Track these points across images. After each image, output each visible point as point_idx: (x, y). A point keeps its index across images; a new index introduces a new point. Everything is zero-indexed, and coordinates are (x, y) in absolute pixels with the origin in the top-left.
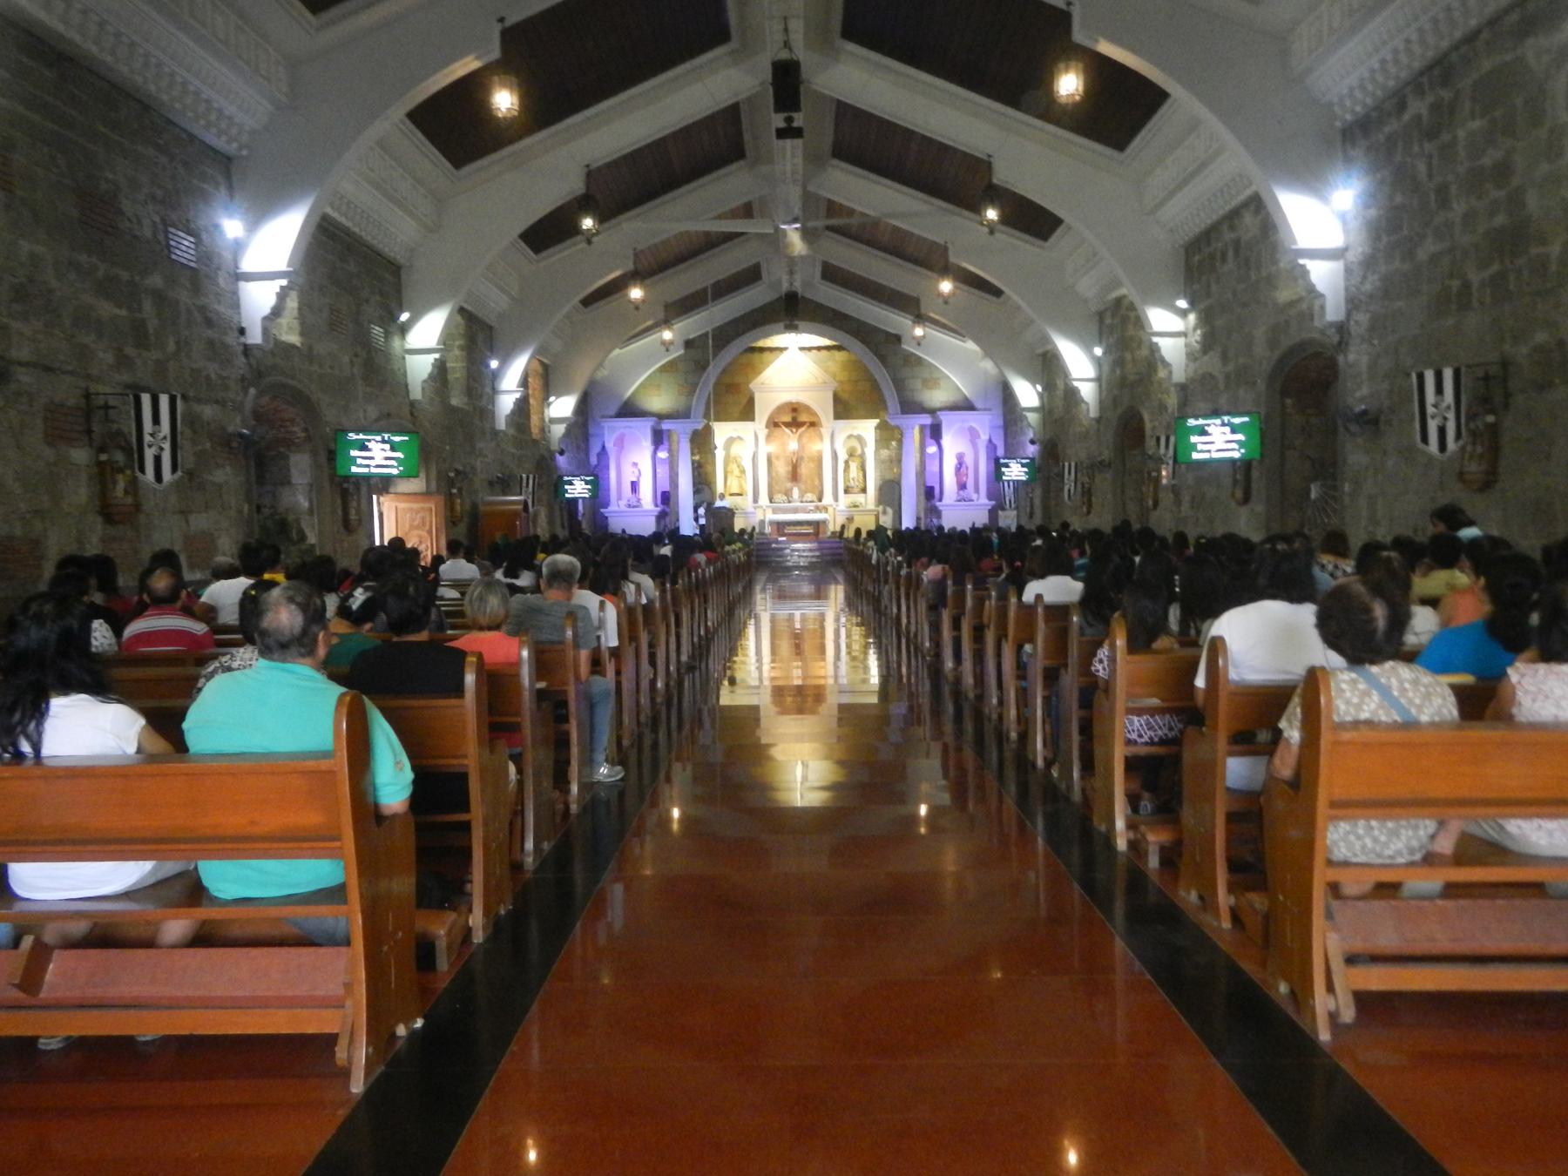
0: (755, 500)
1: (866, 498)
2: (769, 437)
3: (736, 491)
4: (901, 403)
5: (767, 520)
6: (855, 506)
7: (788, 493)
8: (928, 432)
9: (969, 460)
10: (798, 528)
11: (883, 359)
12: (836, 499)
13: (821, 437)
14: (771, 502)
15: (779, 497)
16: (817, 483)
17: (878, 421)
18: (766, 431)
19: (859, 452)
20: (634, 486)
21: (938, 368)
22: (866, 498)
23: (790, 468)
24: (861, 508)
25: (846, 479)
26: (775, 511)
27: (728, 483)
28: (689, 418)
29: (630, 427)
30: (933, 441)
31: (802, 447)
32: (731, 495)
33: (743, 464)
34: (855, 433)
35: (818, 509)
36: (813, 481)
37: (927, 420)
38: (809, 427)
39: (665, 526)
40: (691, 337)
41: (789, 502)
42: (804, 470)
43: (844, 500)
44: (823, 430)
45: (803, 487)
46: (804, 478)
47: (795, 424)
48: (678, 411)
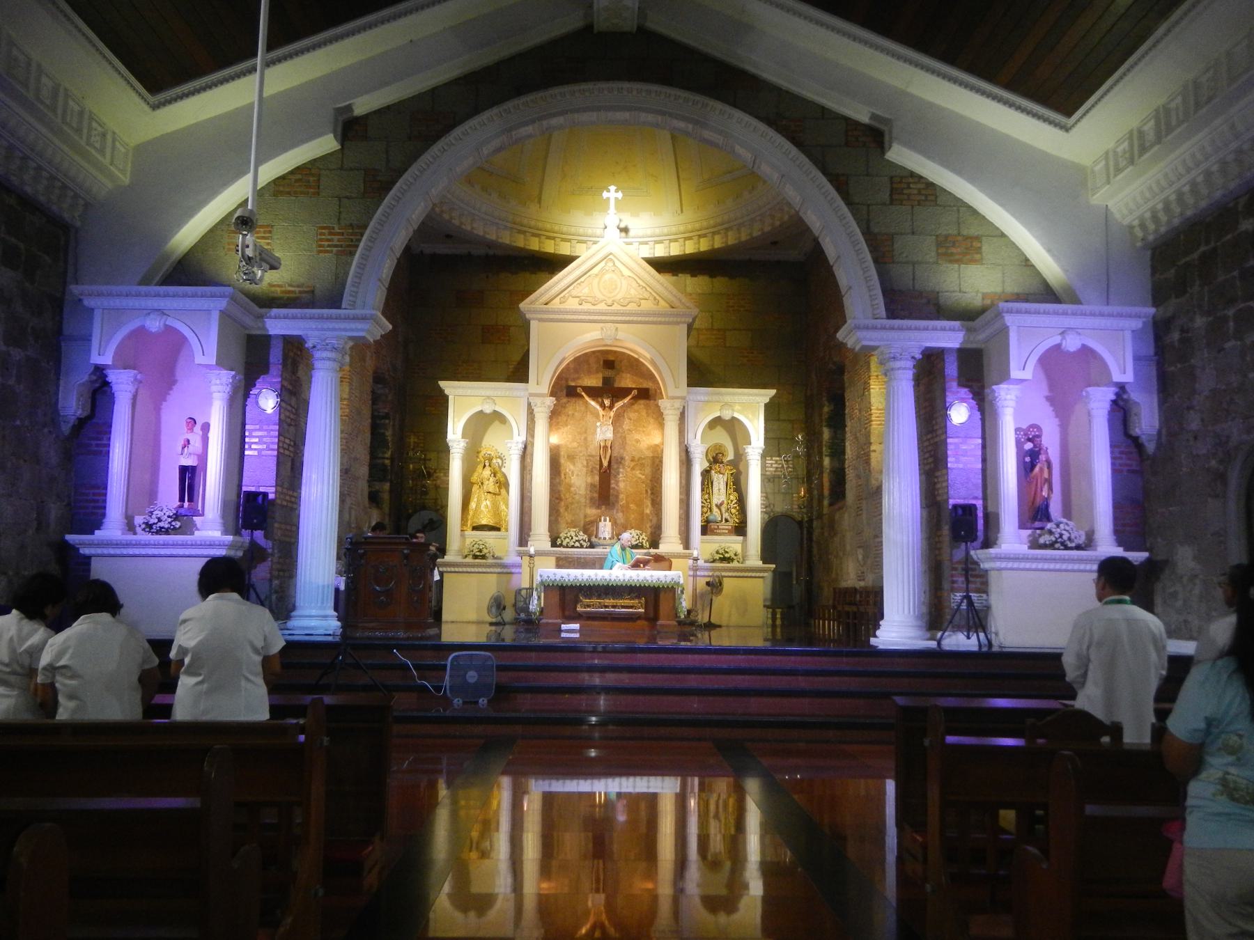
0: (523, 540)
1: (744, 544)
2: (555, 416)
3: (491, 523)
4: (885, 292)
5: (537, 579)
6: (723, 559)
7: (589, 528)
8: (951, 368)
9: (1051, 442)
11: (841, 184)
12: (687, 543)
13: (660, 418)
14: (554, 544)
15: (570, 534)
16: (648, 511)
17: (773, 392)
18: (550, 401)
19: (730, 456)
20: (189, 478)
21: (974, 212)
22: (744, 544)
24: (735, 564)
25: (707, 506)
26: (562, 562)
27: (473, 505)
28: (339, 307)
29: (161, 312)
30: (964, 392)
32: (475, 528)
34: (727, 415)
36: (640, 504)
37: (948, 337)
38: (635, 398)
40: (363, 105)
41: (592, 546)
42: (625, 483)
43: (703, 547)
44: (660, 402)
45: (620, 516)
46: (621, 496)
47: (609, 392)
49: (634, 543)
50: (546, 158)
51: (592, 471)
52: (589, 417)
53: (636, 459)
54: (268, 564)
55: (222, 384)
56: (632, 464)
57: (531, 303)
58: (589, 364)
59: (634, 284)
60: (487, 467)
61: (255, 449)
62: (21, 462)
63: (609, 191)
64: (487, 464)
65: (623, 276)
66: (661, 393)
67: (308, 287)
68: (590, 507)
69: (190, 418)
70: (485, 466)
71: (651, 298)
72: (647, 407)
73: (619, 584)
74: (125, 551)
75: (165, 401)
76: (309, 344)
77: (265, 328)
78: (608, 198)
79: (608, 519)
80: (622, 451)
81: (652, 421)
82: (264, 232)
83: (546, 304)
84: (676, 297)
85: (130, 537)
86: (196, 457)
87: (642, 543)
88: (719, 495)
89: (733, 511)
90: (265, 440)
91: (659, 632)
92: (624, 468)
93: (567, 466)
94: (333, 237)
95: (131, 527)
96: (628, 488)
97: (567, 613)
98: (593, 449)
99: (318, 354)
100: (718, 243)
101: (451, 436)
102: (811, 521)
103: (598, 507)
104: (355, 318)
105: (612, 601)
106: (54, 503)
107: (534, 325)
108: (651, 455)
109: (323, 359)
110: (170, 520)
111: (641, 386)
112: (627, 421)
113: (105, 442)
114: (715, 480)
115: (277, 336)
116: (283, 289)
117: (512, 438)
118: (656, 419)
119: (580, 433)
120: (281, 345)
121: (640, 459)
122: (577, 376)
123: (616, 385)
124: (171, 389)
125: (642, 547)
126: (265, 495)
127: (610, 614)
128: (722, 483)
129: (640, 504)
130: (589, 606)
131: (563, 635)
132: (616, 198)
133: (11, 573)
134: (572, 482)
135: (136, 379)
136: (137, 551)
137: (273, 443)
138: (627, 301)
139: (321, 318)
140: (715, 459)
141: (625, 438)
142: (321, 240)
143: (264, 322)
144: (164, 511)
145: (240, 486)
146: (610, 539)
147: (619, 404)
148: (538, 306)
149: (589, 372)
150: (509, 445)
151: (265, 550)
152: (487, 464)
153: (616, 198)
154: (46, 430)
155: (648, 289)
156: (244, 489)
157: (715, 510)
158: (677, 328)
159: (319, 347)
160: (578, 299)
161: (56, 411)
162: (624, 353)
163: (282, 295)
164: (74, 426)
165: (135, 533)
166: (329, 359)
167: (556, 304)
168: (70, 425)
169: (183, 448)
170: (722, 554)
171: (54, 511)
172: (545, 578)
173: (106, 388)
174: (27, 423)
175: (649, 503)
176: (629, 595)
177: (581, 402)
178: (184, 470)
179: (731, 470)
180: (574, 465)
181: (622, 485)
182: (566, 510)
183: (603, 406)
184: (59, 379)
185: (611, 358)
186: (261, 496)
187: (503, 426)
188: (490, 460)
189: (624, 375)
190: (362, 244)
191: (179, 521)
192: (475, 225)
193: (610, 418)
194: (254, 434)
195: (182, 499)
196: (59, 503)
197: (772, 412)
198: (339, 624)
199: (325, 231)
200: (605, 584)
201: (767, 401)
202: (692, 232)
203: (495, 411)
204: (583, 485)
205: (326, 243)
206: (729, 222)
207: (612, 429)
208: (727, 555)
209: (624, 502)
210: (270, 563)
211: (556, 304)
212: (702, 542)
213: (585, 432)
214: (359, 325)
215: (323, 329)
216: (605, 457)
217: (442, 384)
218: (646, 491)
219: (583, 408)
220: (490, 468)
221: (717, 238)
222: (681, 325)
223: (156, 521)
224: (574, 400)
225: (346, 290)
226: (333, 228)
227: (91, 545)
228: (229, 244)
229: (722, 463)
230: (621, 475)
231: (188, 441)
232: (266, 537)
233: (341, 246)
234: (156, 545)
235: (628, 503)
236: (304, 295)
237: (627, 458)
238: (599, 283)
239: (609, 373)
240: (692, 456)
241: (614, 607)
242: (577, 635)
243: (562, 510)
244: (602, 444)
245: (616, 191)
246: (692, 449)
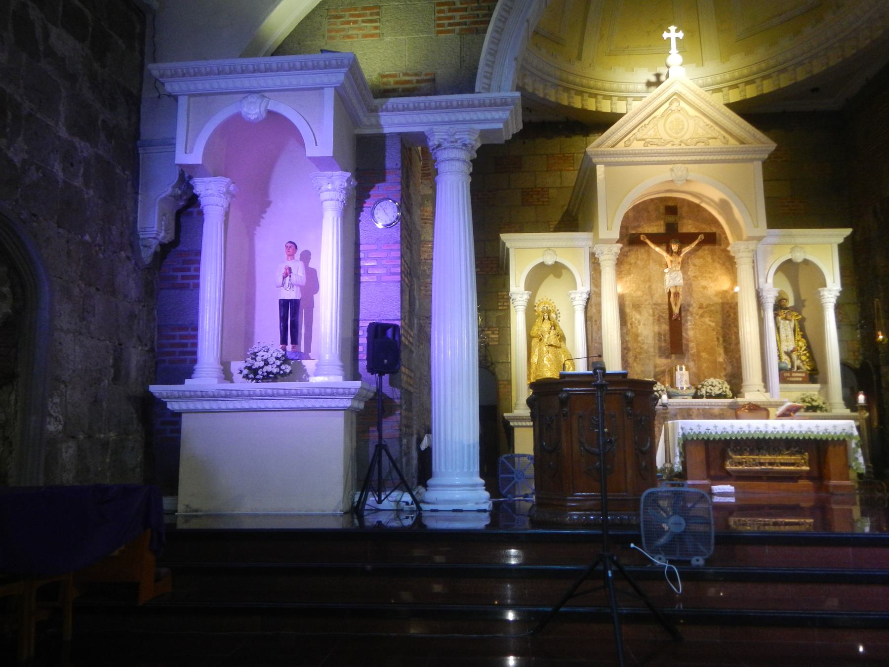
2: (620, 262)
10: (768, 458)
13: (730, 264)
16: (721, 359)
17: (848, 232)
18: (617, 248)
19: (791, 303)
23: (665, 327)
27: (535, 359)
28: (472, 91)
31: (688, 285)
33: (563, 325)
34: (798, 257)
35: (735, 412)
38: (700, 244)
39: (381, 447)
42: (692, 332)
46: (691, 345)
48: (434, 80)
49: (718, 392)
50: (585, 19)
51: (659, 320)
52: (653, 267)
53: (704, 305)
54: (396, 417)
55: (335, 190)
56: (701, 311)
57: (598, 147)
58: (649, 212)
59: (702, 124)
60: (546, 321)
61: (373, 274)
62: (93, 290)
63: (669, 31)
64: (546, 317)
65: (688, 114)
66: (726, 238)
67: (427, 75)
68: (660, 356)
69: (290, 242)
70: (544, 319)
71: (722, 137)
72: (713, 253)
73: (778, 437)
74: (223, 405)
75: (259, 226)
76: (433, 142)
77: (379, 126)
78: (669, 39)
79: (684, 367)
80: (688, 298)
81: (718, 266)
82: (371, 14)
83: (613, 146)
84: (750, 133)
85: (228, 386)
86: (299, 288)
87: (725, 392)
88: (787, 342)
89: (804, 358)
90: (384, 262)
91: (832, 494)
92: (692, 314)
93: (634, 316)
94: (454, 13)
95: (227, 376)
96: (698, 335)
97: (712, 473)
98: (660, 296)
99: (442, 155)
100: (785, 81)
101: (513, 288)
102: (878, 367)
103: (668, 357)
104: (494, 105)
105: (768, 457)
106: (134, 347)
107: (600, 170)
108: (720, 301)
109: (453, 159)
110: (278, 363)
111: (708, 231)
112: (691, 268)
113: (193, 273)
114: (781, 326)
115: (392, 135)
116: (397, 79)
117: (575, 288)
118: (723, 264)
119: (644, 281)
120: (398, 146)
121: (708, 306)
122: (636, 224)
123: (680, 231)
124: (265, 212)
125: (725, 397)
126: (395, 328)
127: (766, 472)
128: (789, 329)
129: (711, 352)
130: (740, 464)
131: (716, 499)
132: (677, 38)
133: (81, 437)
134: (639, 331)
135: (228, 192)
136: (238, 405)
137: (394, 266)
138: (694, 141)
139: (449, 107)
140: (779, 306)
141: (691, 285)
142: (440, 19)
143: (379, 116)
144: (271, 352)
145: (356, 321)
146: (688, 388)
147: (687, 249)
148: (603, 149)
149: (649, 220)
150: (572, 296)
151: (391, 400)
152: (546, 317)
153: (677, 38)
154: (123, 254)
155: (717, 128)
156: (364, 325)
157: (785, 358)
158: (750, 165)
159: (446, 144)
160: (643, 142)
161: (134, 232)
162: (684, 200)
163: (396, 86)
164: (156, 253)
165: (232, 382)
166: (458, 160)
167: (621, 146)
168: (153, 250)
169: (284, 278)
170: (809, 402)
171: (135, 357)
172: (687, 431)
173: (194, 210)
174: (99, 239)
175: (721, 350)
176: (788, 449)
177: (643, 250)
178: (285, 305)
179: (797, 316)
180: (640, 313)
181: (691, 333)
182: (635, 360)
183: (669, 251)
184: (137, 193)
185: (670, 204)
186: (390, 332)
187: (556, 280)
188: (549, 312)
189: (685, 221)
190: (495, 14)
191: (289, 364)
192: (526, 81)
193: (679, 263)
194: (371, 255)
195: (284, 341)
196: (140, 348)
197: (844, 249)
198: (487, 494)
199: (445, 8)
200: (761, 437)
201: (841, 240)
202: (740, 78)
203: (556, 262)
204: (651, 335)
205: (446, 22)
206: (784, 63)
207: (681, 274)
208: (815, 404)
209: (695, 350)
210: (399, 417)
211: (621, 146)
212: (781, 390)
213: (649, 280)
214: (496, 115)
215: (450, 123)
216: (676, 304)
217: (504, 237)
218: (718, 339)
219: (645, 256)
220: (549, 322)
221: (765, 82)
222: (756, 163)
223: (262, 364)
224: (635, 248)
225: (479, 71)
226: (454, 3)
227: (180, 397)
228: (330, 31)
229: (787, 309)
230: (689, 323)
231: (290, 269)
232: (392, 383)
233: (465, 24)
234: (264, 396)
235: (698, 352)
236: (423, 85)
237: (694, 305)
238: (665, 123)
239: (671, 219)
240: (764, 301)
241: (771, 464)
242: (732, 500)
243: (630, 360)
244: (673, 291)
245: (677, 31)
246: (764, 294)
